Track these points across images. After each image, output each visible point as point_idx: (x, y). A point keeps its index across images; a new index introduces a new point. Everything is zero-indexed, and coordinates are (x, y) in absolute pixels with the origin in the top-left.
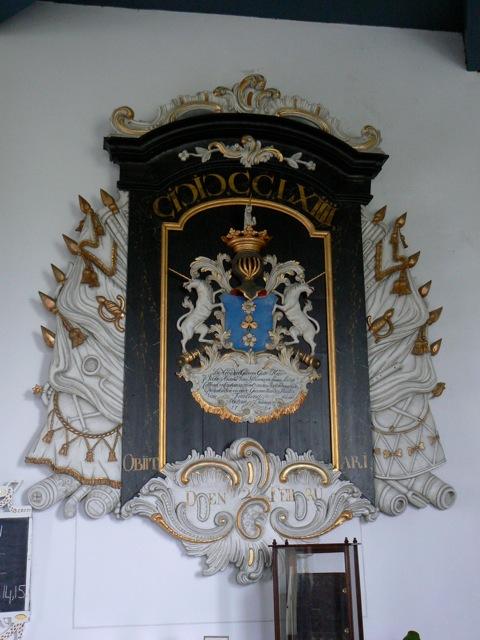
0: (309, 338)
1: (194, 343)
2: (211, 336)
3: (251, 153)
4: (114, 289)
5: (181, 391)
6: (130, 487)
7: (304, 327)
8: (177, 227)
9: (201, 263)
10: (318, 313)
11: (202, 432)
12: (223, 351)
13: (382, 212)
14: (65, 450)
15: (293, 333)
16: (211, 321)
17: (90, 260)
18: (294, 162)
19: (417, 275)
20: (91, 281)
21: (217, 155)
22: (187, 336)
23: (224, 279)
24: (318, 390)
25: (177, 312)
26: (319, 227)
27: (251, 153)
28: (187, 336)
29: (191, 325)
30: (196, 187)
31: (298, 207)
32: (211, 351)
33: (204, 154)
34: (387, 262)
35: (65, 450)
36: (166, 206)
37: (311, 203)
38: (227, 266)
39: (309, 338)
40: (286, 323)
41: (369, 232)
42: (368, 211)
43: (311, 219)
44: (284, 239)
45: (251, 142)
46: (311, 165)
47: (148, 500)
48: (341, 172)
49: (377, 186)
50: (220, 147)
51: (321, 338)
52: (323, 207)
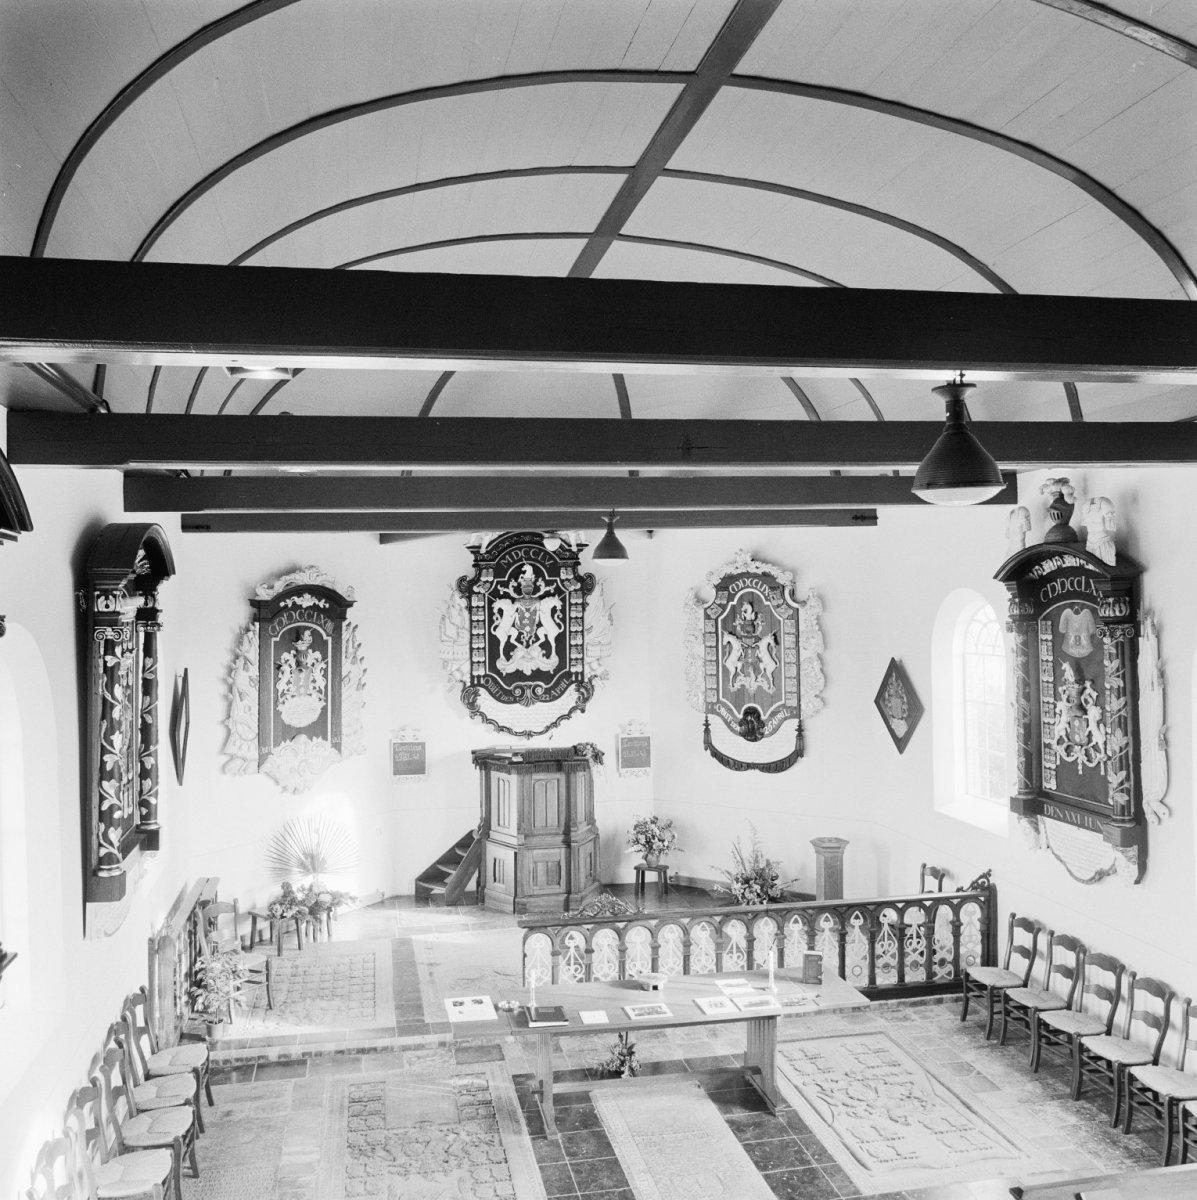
0: (323, 688)
1: (283, 694)
2: (288, 690)
3: (307, 601)
4: (254, 671)
5: (278, 714)
6: (262, 759)
7: (321, 683)
8: (278, 639)
9: (285, 656)
10: (325, 676)
11: (289, 733)
12: (293, 696)
13: (349, 625)
14: (240, 748)
15: (317, 685)
16: (289, 683)
17: (246, 659)
18: (321, 604)
19: (360, 655)
20: (245, 668)
21: (294, 604)
22: (280, 691)
23: (293, 662)
24: (324, 709)
25: (277, 680)
26: (328, 636)
27: (307, 601)
28: (280, 691)
29: (282, 686)
30: (284, 620)
31: (320, 626)
32: (289, 697)
33: (289, 603)
34: (351, 650)
35: (240, 748)
36: (274, 628)
37: (325, 623)
38: (295, 656)
39: (323, 688)
40: (314, 681)
41: (345, 635)
42: (344, 624)
43: (325, 631)
44: (318, 644)
45: (307, 596)
46: (327, 606)
47: (266, 766)
48: (335, 605)
49: (349, 611)
50: (296, 598)
51: (326, 687)
52: (330, 625)
